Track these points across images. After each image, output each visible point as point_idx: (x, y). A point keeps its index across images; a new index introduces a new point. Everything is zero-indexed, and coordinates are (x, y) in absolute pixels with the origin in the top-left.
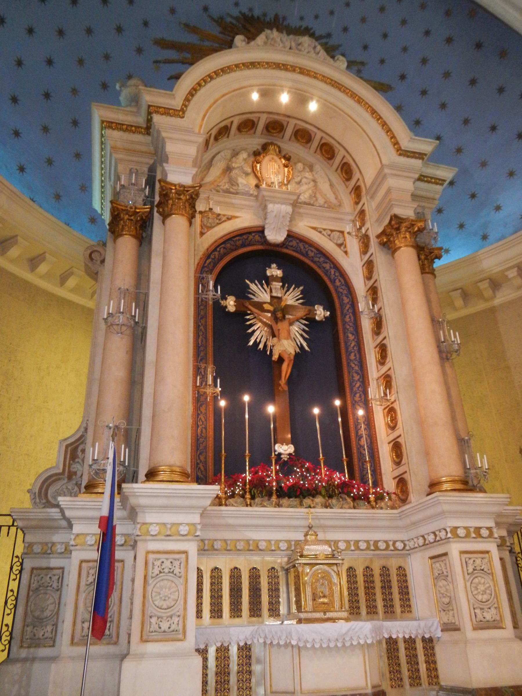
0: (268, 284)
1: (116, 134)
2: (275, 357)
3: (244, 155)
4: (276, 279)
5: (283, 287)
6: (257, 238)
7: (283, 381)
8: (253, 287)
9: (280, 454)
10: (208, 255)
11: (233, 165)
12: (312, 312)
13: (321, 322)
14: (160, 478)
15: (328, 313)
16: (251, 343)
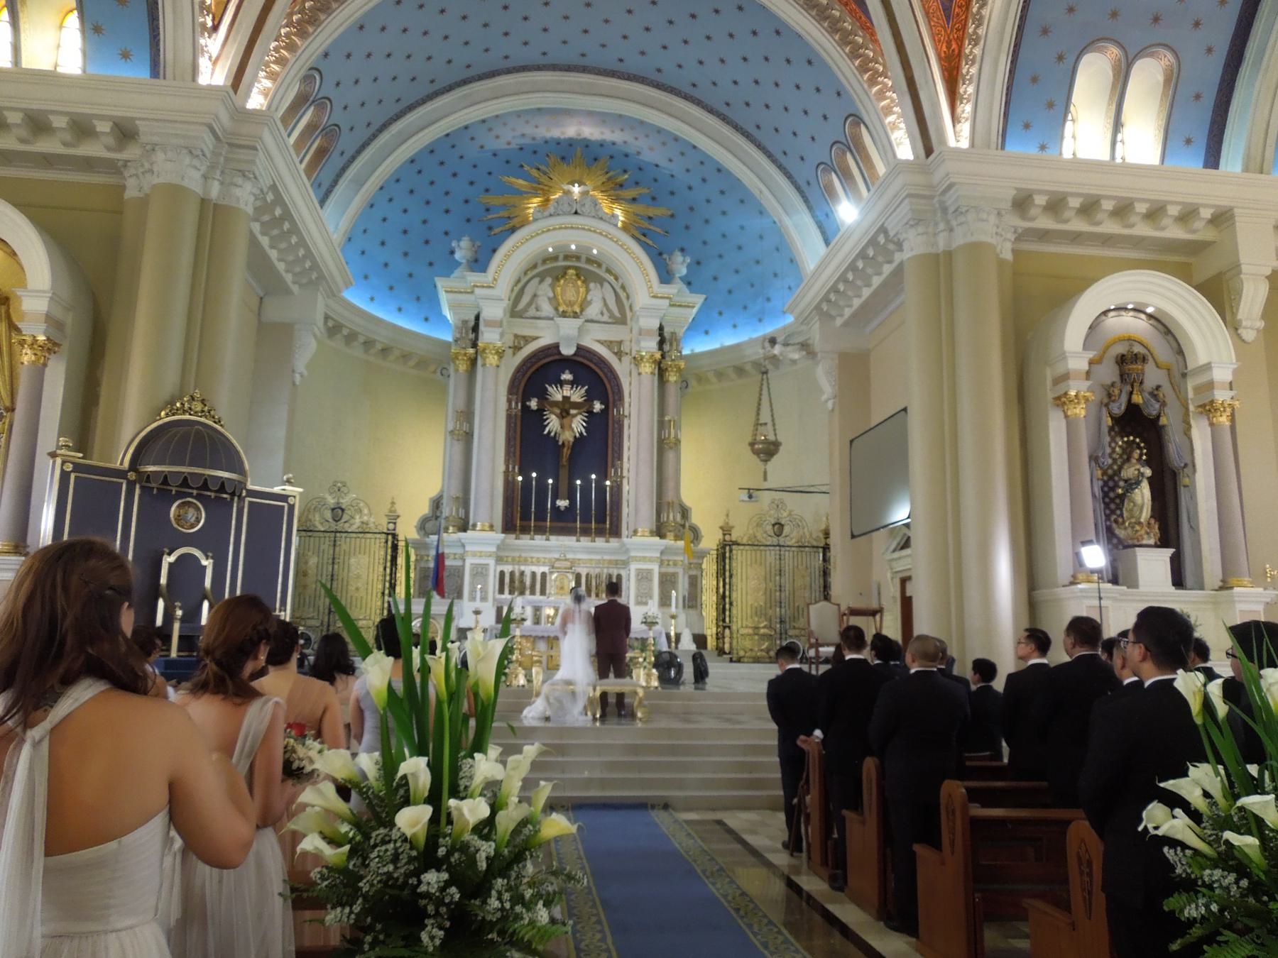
0: (561, 387)
1: (451, 296)
2: (560, 443)
3: (549, 280)
4: (567, 382)
5: (572, 388)
6: (555, 351)
7: (564, 461)
8: (550, 389)
9: (559, 507)
10: (518, 370)
11: (540, 293)
12: (592, 406)
13: (598, 413)
14: (478, 529)
15: (603, 407)
16: (546, 432)
